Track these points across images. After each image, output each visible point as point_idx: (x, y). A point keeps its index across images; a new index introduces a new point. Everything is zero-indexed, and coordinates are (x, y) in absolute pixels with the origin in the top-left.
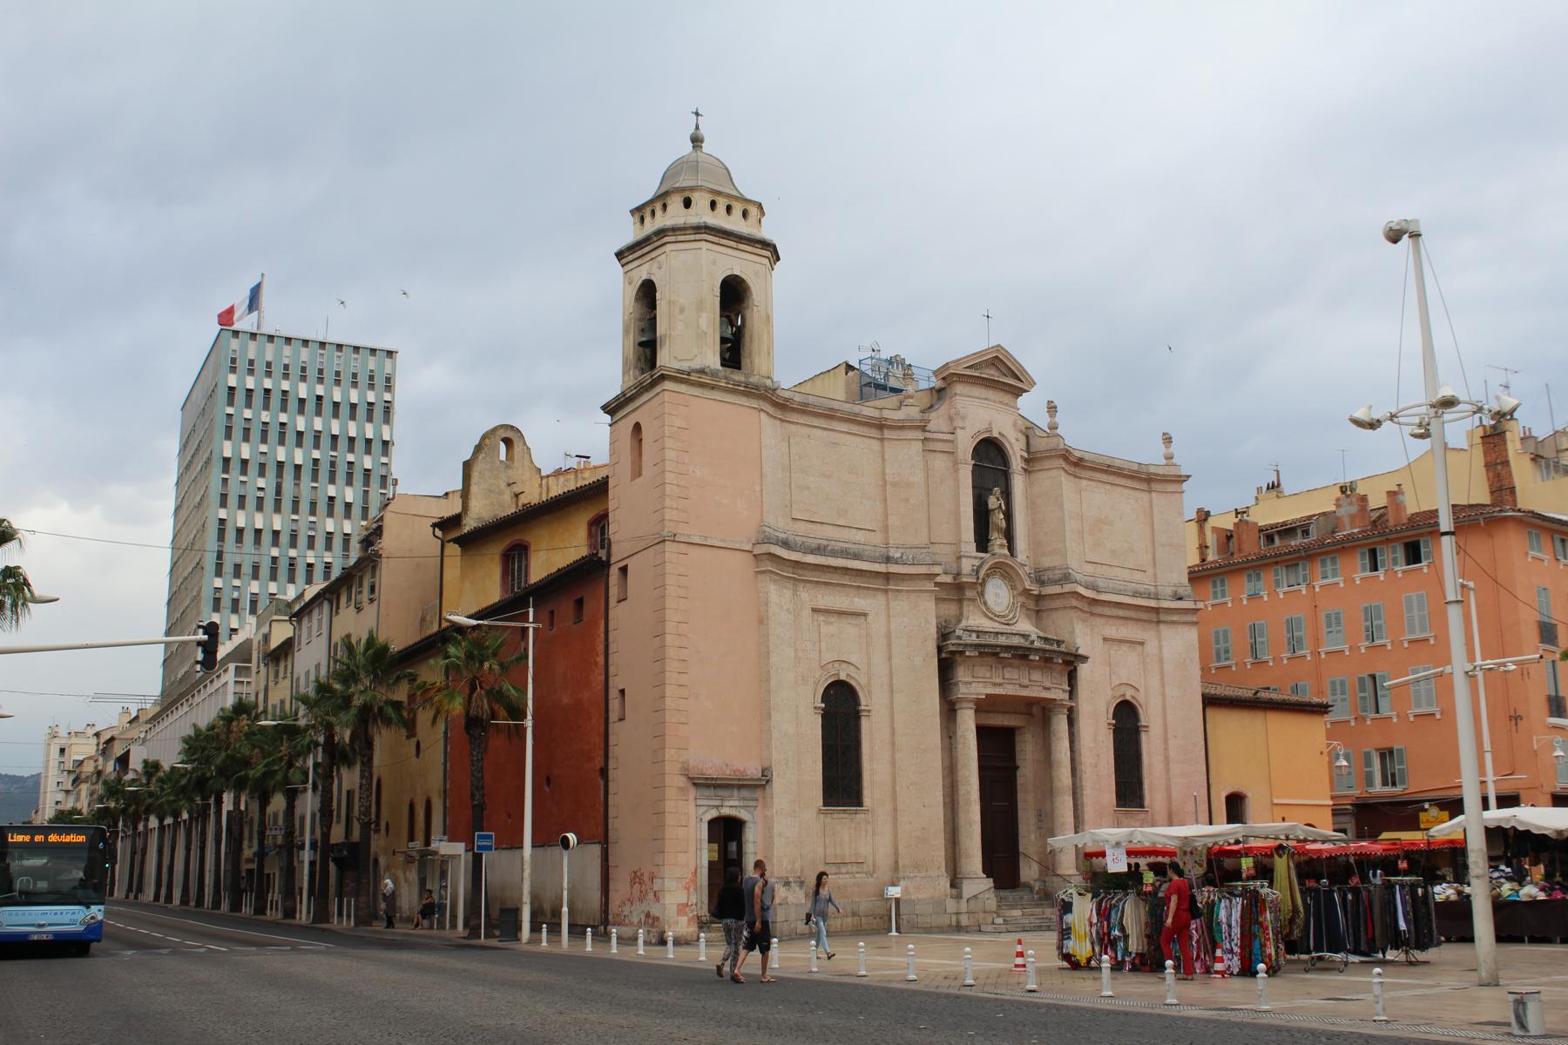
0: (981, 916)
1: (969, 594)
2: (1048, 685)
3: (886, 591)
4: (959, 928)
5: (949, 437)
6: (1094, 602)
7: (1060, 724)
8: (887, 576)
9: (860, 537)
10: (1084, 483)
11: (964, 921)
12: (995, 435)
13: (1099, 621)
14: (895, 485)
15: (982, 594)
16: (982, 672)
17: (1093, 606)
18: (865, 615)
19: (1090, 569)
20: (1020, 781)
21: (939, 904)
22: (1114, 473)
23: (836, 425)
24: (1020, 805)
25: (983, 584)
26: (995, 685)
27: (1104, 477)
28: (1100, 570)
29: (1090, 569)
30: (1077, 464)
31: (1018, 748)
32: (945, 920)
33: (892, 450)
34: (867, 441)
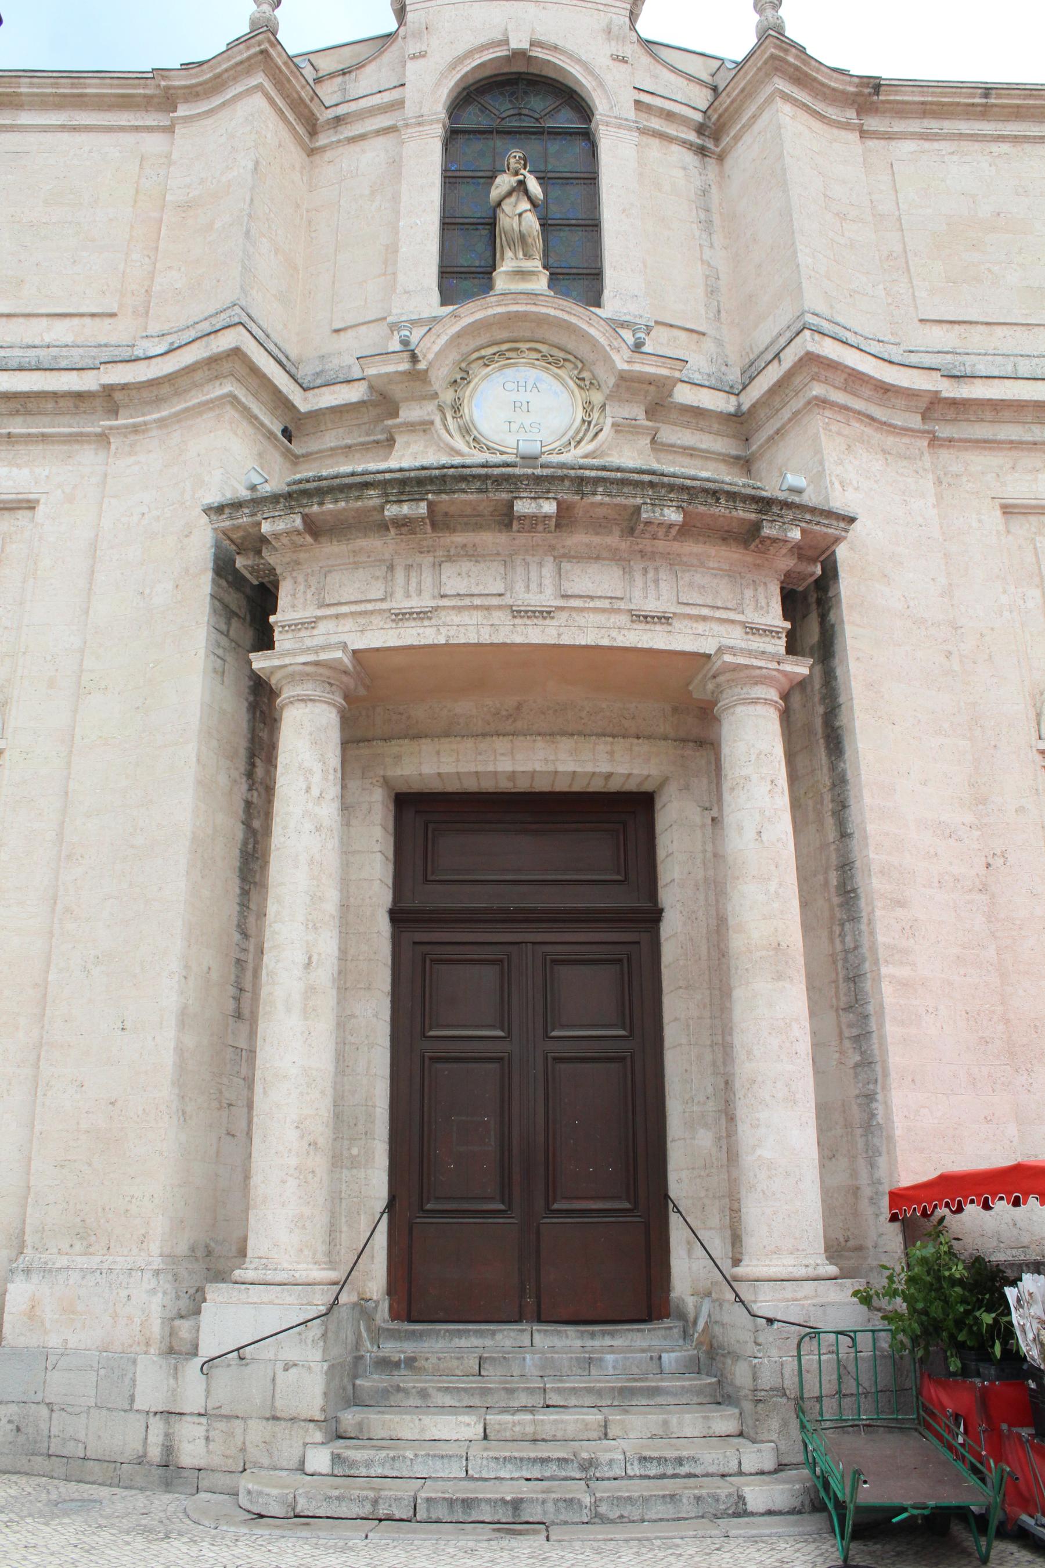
0: (257, 1431)
1: (410, 413)
2: (652, 606)
3: (103, 439)
4: (169, 1472)
5: (395, 95)
6: (934, 406)
7: (755, 742)
8: (109, 399)
9: (61, 332)
10: (908, 146)
11: (192, 1449)
12: (519, 42)
13: (979, 461)
14: (186, 206)
15: (456, 408)
16: (352, 586)
17: (942, 416)
18: (30, 506)
19: (940, 337)
20: (669, 952)
21: (116, 1366)
22: (1018, 113)
23: (26, 118)
24: (672, 1033)
25: (461, 380)
26: (401, 617)
27: (987, 128)
28: (977, 339)
29: (940, 337)
30: (869, 101)
31: (661, 853)
32: (128, 1437)
33: (185, 139)
34: (130, 138)
